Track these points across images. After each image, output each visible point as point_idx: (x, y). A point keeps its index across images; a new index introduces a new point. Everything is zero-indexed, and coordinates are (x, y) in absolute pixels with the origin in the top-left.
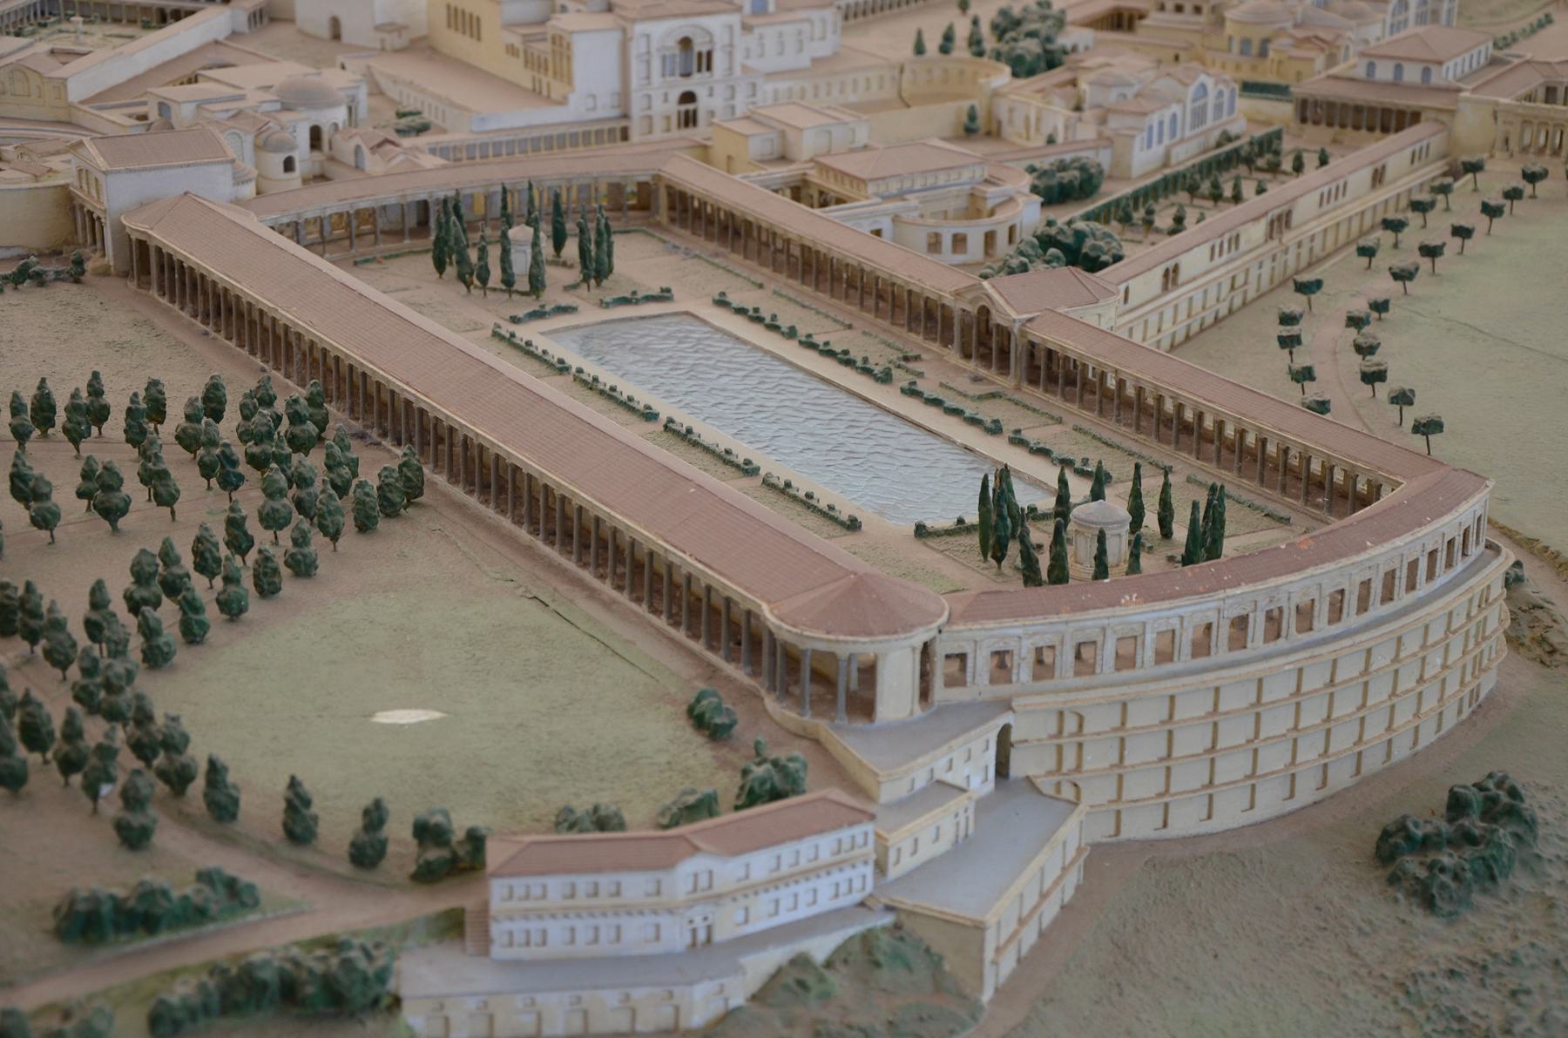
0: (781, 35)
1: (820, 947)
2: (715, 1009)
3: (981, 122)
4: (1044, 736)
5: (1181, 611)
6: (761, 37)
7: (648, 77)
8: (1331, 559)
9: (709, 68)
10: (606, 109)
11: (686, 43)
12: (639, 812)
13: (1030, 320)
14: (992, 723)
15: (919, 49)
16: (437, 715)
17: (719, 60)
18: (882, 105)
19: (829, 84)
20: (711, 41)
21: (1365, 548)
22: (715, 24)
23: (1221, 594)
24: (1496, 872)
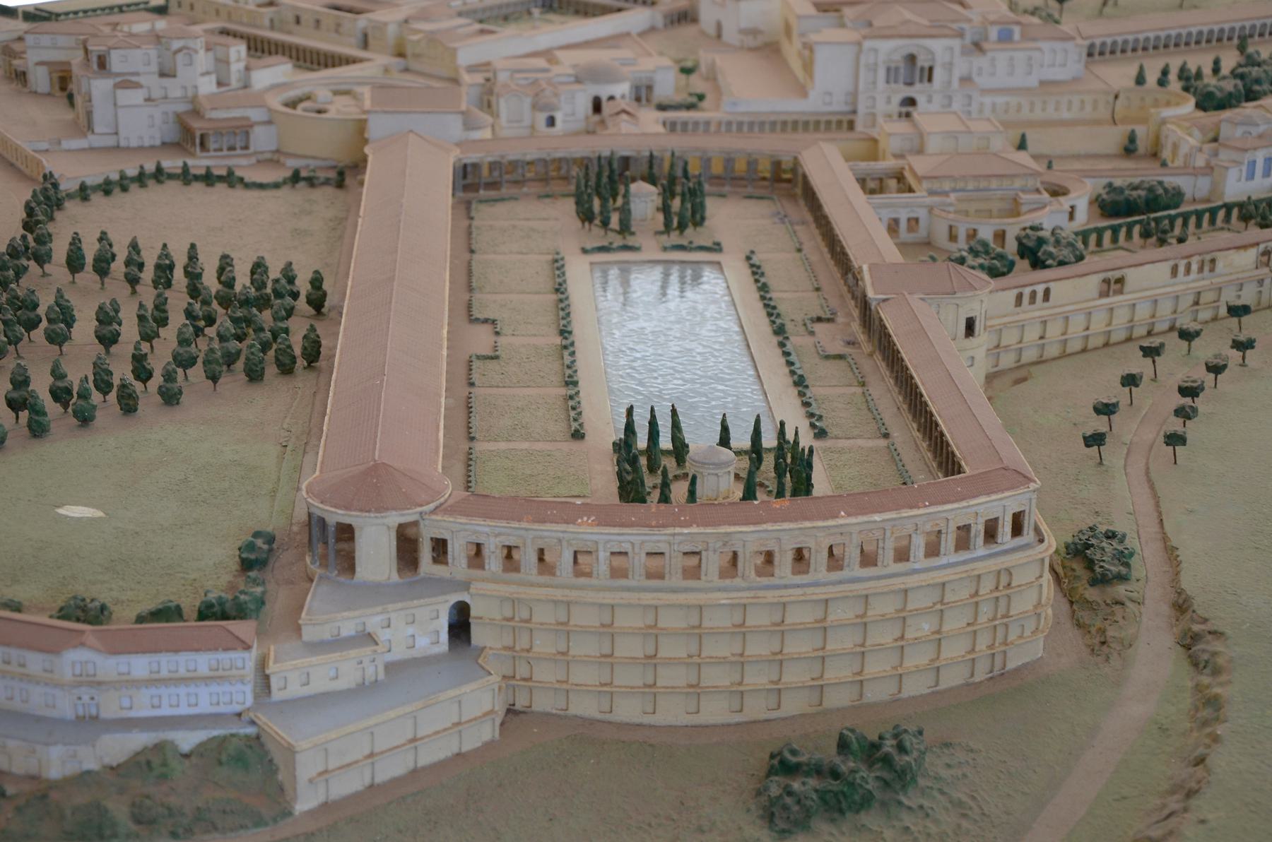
0: (1012, 59)
1: (187, 740)
2: (71, 769)
3: (1142, 145)
4: (498, 617)
5: (632, 538)
6: (993, 59)
7: (874, 83)
8: (795, 520)
9: (930, 80)
10: (839, 105)
11: (912, 59)
12: (124, 615)
13: (885, 300)
14: (447, 597)
15: (1140, 80)
16: (99, 514)
17: (938, 74)
18: (1097, 122)
19: (1045, 102)
20: (933, 59)
21: (836, 516)
22: (937, 45)
23: (670, 530)
24: (844, 805)
